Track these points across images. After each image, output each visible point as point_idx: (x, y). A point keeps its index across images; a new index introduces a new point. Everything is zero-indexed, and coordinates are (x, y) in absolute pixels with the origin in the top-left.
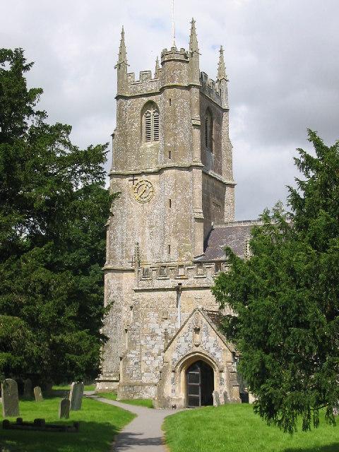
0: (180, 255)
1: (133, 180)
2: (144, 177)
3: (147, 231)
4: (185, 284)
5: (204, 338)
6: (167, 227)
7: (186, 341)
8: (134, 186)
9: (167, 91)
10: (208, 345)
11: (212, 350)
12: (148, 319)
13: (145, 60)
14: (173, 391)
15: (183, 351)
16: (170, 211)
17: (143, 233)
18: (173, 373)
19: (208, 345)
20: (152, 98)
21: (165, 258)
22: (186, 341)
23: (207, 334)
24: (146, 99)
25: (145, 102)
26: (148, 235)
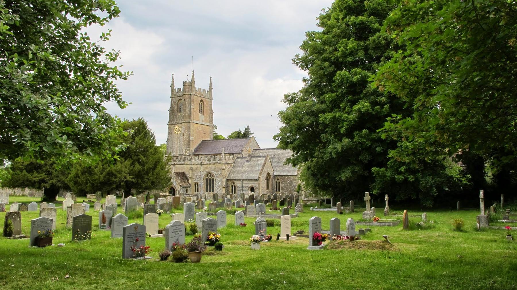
0: (186, 152)
9: (184, 96)
13: (179, 85)
17: (177, 144)
20: (181, 98)
21: (182, 153)
24: (179, 98)
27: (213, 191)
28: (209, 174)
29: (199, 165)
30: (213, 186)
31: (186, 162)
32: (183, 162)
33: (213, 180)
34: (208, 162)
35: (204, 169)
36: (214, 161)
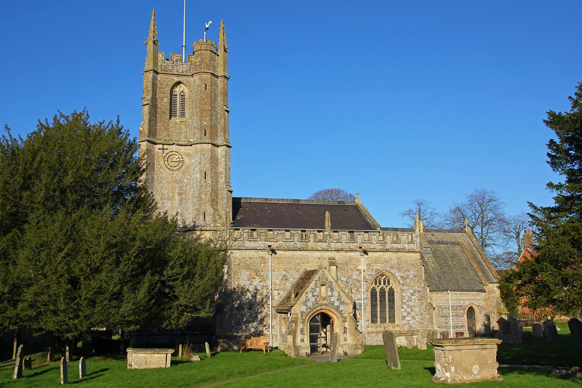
0: (215, 221)
1: (163, 149)
2: (174, 148)
3: (177, 197)
4: (274, 246)
5: (329, 293)
6: (203, 196)
7: (313, 296)
8: (164, 155)
10: (333, 299)
11: (337, 304)
12: (240, 276)
14: (302, 340)
15: (310, 304)
16: (205, 182)
18: (301, 325)
19: (333, 299)
22: (313, 296)
23: (332, 290)
24: (176, 79)
25: (175, 82)
26: (177, 200)
27: (392, 319)
28: (381, 278)
29: (357, 255)
30: (392, 307)
31: (311, 244)
32: (299, 245)
33: (392, 292)
34: (378, 247)
35: (368, 265)
36: (395, 245)
